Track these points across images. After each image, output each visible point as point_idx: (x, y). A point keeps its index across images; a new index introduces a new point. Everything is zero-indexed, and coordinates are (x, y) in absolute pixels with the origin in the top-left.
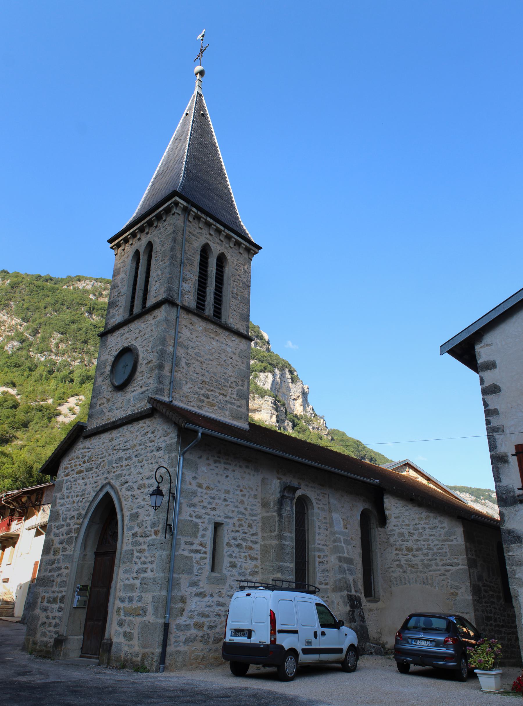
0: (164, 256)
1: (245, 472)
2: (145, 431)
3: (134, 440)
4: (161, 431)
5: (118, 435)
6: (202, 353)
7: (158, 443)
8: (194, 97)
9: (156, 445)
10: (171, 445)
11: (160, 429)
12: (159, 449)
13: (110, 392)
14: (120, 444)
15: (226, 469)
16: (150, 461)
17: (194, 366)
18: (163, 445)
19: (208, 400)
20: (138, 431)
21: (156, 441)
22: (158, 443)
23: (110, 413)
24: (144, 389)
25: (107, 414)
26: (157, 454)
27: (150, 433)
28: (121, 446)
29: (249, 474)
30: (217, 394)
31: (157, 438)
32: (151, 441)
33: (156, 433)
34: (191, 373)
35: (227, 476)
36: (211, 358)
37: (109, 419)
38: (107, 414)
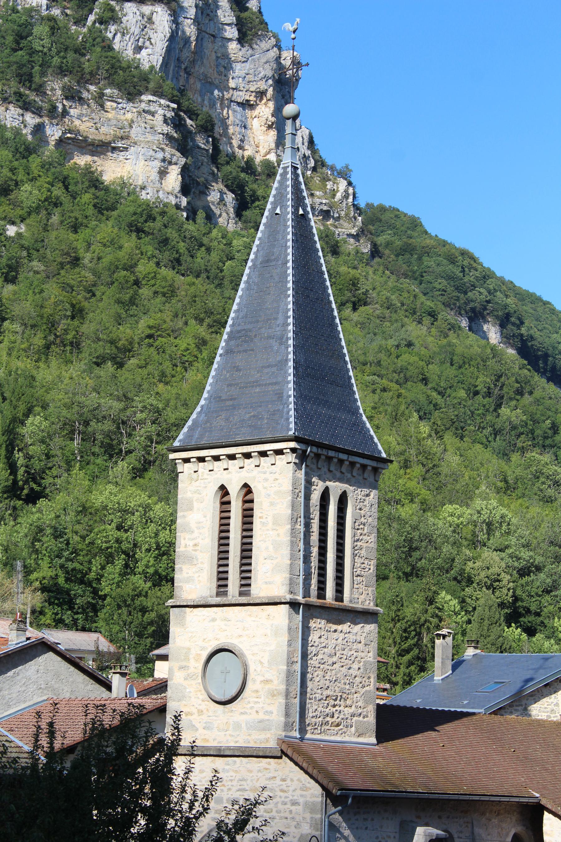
0: (276, 522)
1: (383, 818)
2: (271, 775)
3: (254, 782)
4: (296, 782)
5: (227, 767)
6: (326, 658)
7: (293, 796)
8: (285, 173)
9: (291, 798)
10: (313, 804)
11: (295, 779)
12: (294, 803)
13: (203, 701)
14: (231, 780)
15: (365, 820)
16: (282, 815)
17: (317, 679)
18: (301, 800)
19: (333, 720)
20: (259, 771)
21: (290, 793)
22: (293, 796)
23: (206, 732)
24: (261, 716)
25: (201, 731)
26: (293, 808)
27: (278, 779)
28: (235, 783)
29: (387, 819)
30: (342, 708)
31: (291, 789)
32: (282, 791)
33: (288, 782)
34: (315, 690)
35: (366, 828)
36: (335, 659)
37: (207, 741)
38: (201, 731)
